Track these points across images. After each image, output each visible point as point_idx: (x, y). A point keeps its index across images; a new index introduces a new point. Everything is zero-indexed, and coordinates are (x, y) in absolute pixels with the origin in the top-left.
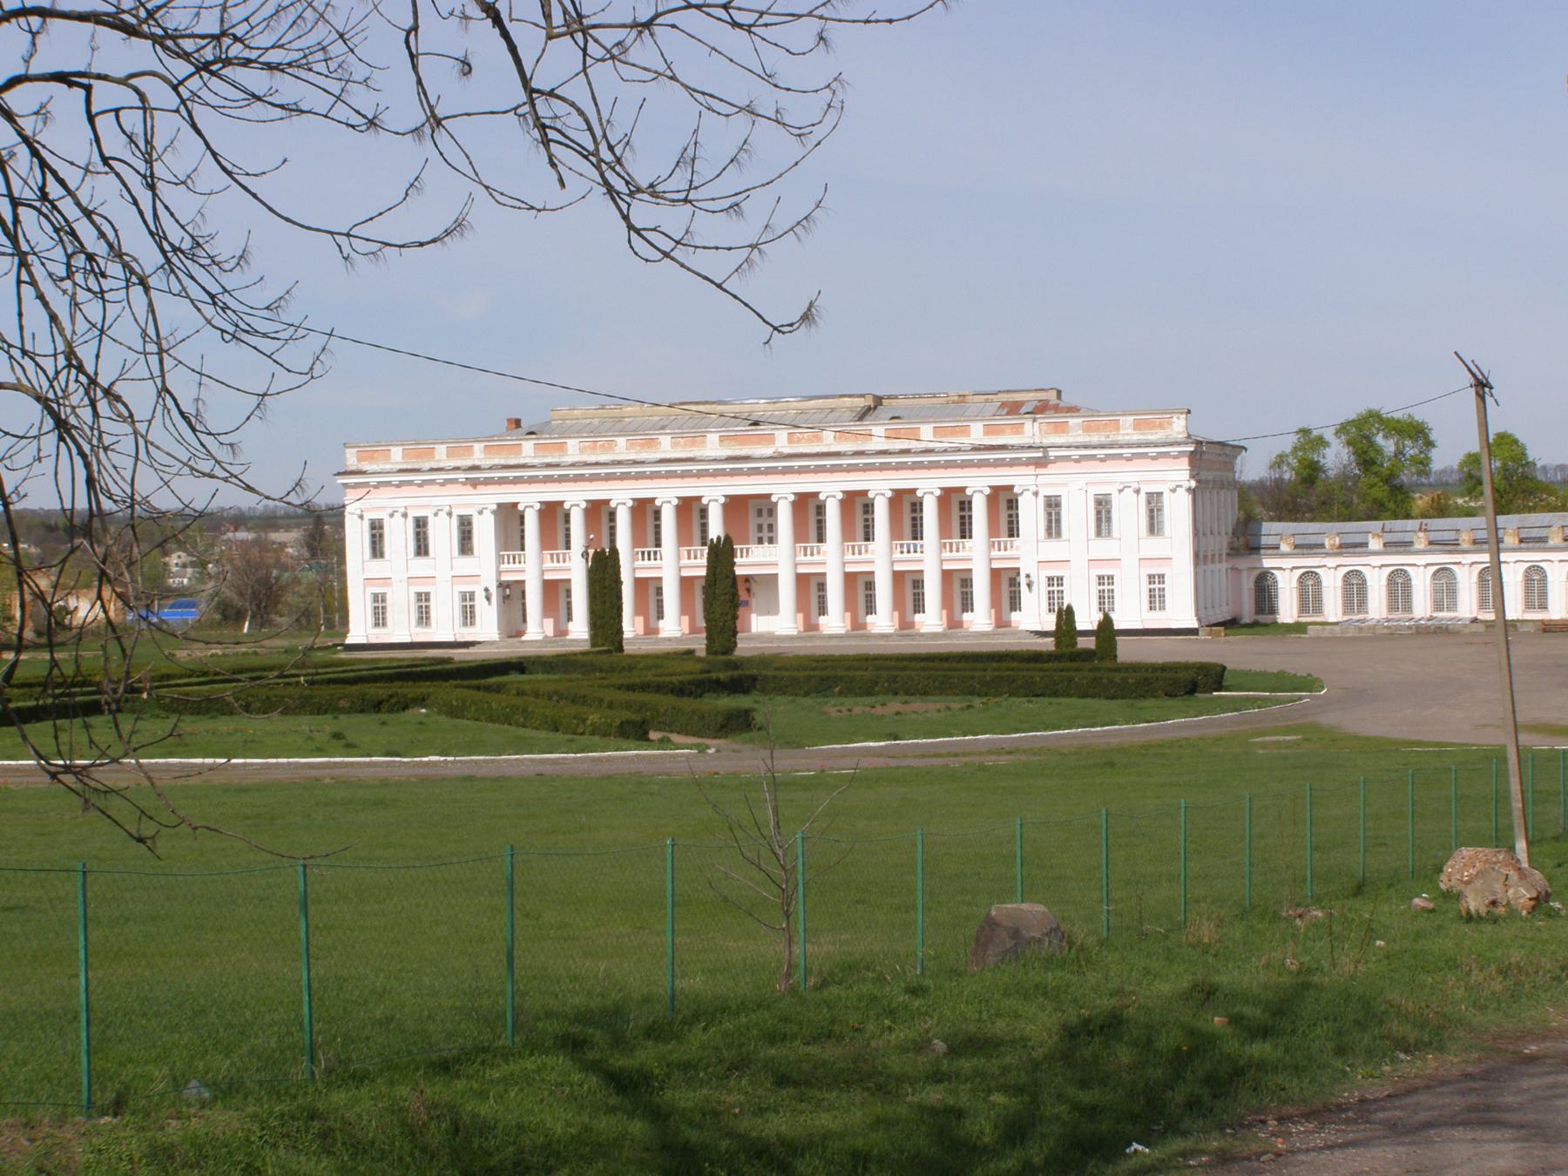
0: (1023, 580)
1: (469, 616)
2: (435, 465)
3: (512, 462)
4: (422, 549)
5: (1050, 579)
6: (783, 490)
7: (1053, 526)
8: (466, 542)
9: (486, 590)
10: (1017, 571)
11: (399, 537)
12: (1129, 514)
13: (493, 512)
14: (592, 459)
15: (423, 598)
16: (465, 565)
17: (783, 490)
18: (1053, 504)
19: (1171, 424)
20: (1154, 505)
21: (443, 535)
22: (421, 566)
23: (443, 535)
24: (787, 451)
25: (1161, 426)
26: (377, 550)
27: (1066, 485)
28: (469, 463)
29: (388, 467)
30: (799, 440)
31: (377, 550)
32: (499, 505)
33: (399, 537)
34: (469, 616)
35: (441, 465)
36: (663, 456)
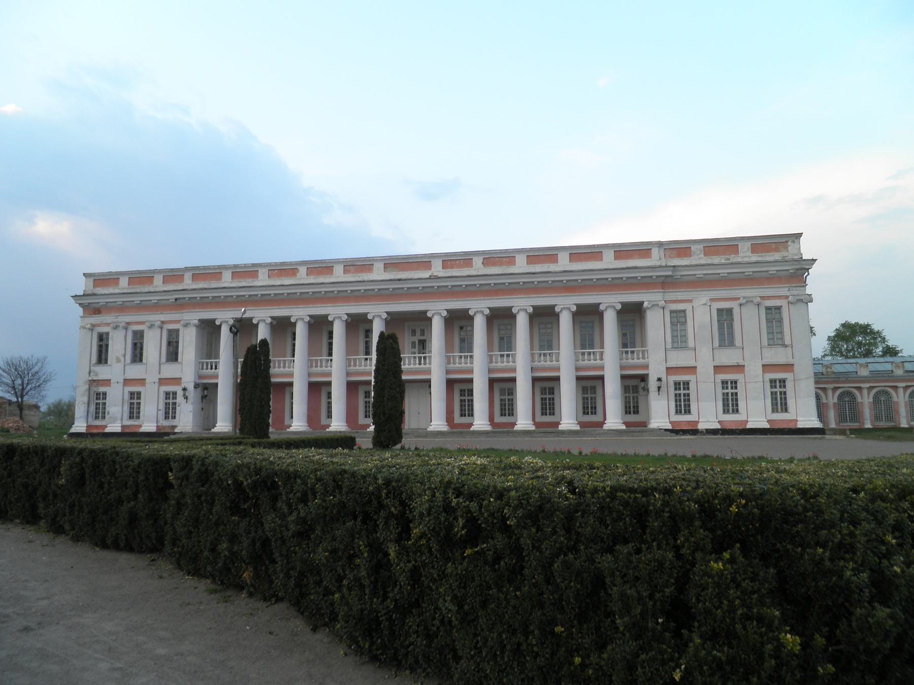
0: (652, 383)
1: (170, 411)
2: (152, 289)
3: (214, 284)
4: (138, 355)
5: (677, 385)
6: (437, 309)
7: (679, 341)
8: (173, 355)
9: (185, 389)
10: (644, 378)
11: (119, 345)
12: (750, 324)
13: (197, 326)
14: (278, 282)
15: (135, 396)
16: (170, 371)
17: (437, 309)
18: (678, 319)
19: (786, 248)
20: (774, 315)
21: (154, 347)
22: (135, 371)
23: (154, 347)
24: (440, 275)
25: (777, 250)
26: (102, 357)
27: (691, 301)
28: (180, 287)
29: (117, 291)
30: (452, 267)
31: (102, 357)
32: (200, 320)
33: (119, 345)
34: (170, 411)
35: (157, 289)
36: (336, 280)
